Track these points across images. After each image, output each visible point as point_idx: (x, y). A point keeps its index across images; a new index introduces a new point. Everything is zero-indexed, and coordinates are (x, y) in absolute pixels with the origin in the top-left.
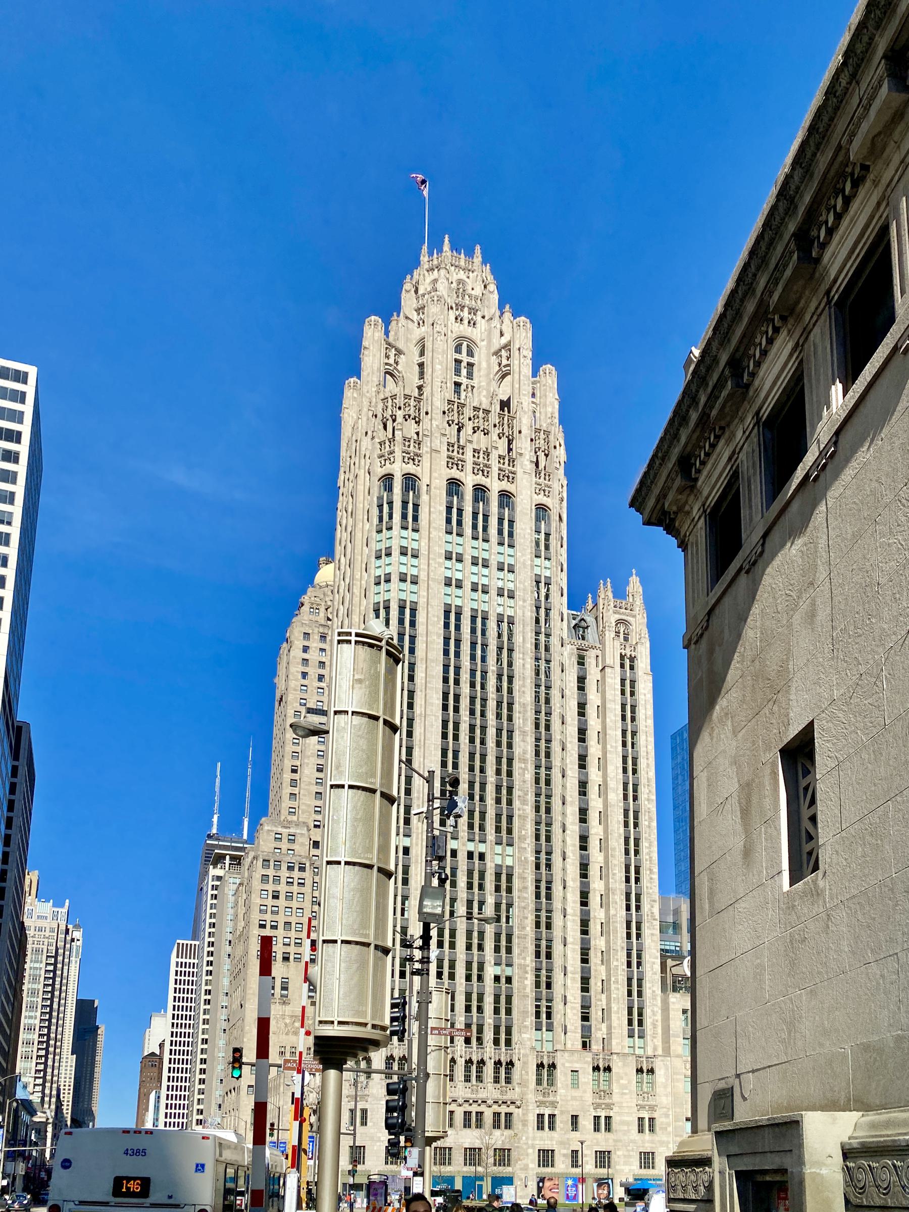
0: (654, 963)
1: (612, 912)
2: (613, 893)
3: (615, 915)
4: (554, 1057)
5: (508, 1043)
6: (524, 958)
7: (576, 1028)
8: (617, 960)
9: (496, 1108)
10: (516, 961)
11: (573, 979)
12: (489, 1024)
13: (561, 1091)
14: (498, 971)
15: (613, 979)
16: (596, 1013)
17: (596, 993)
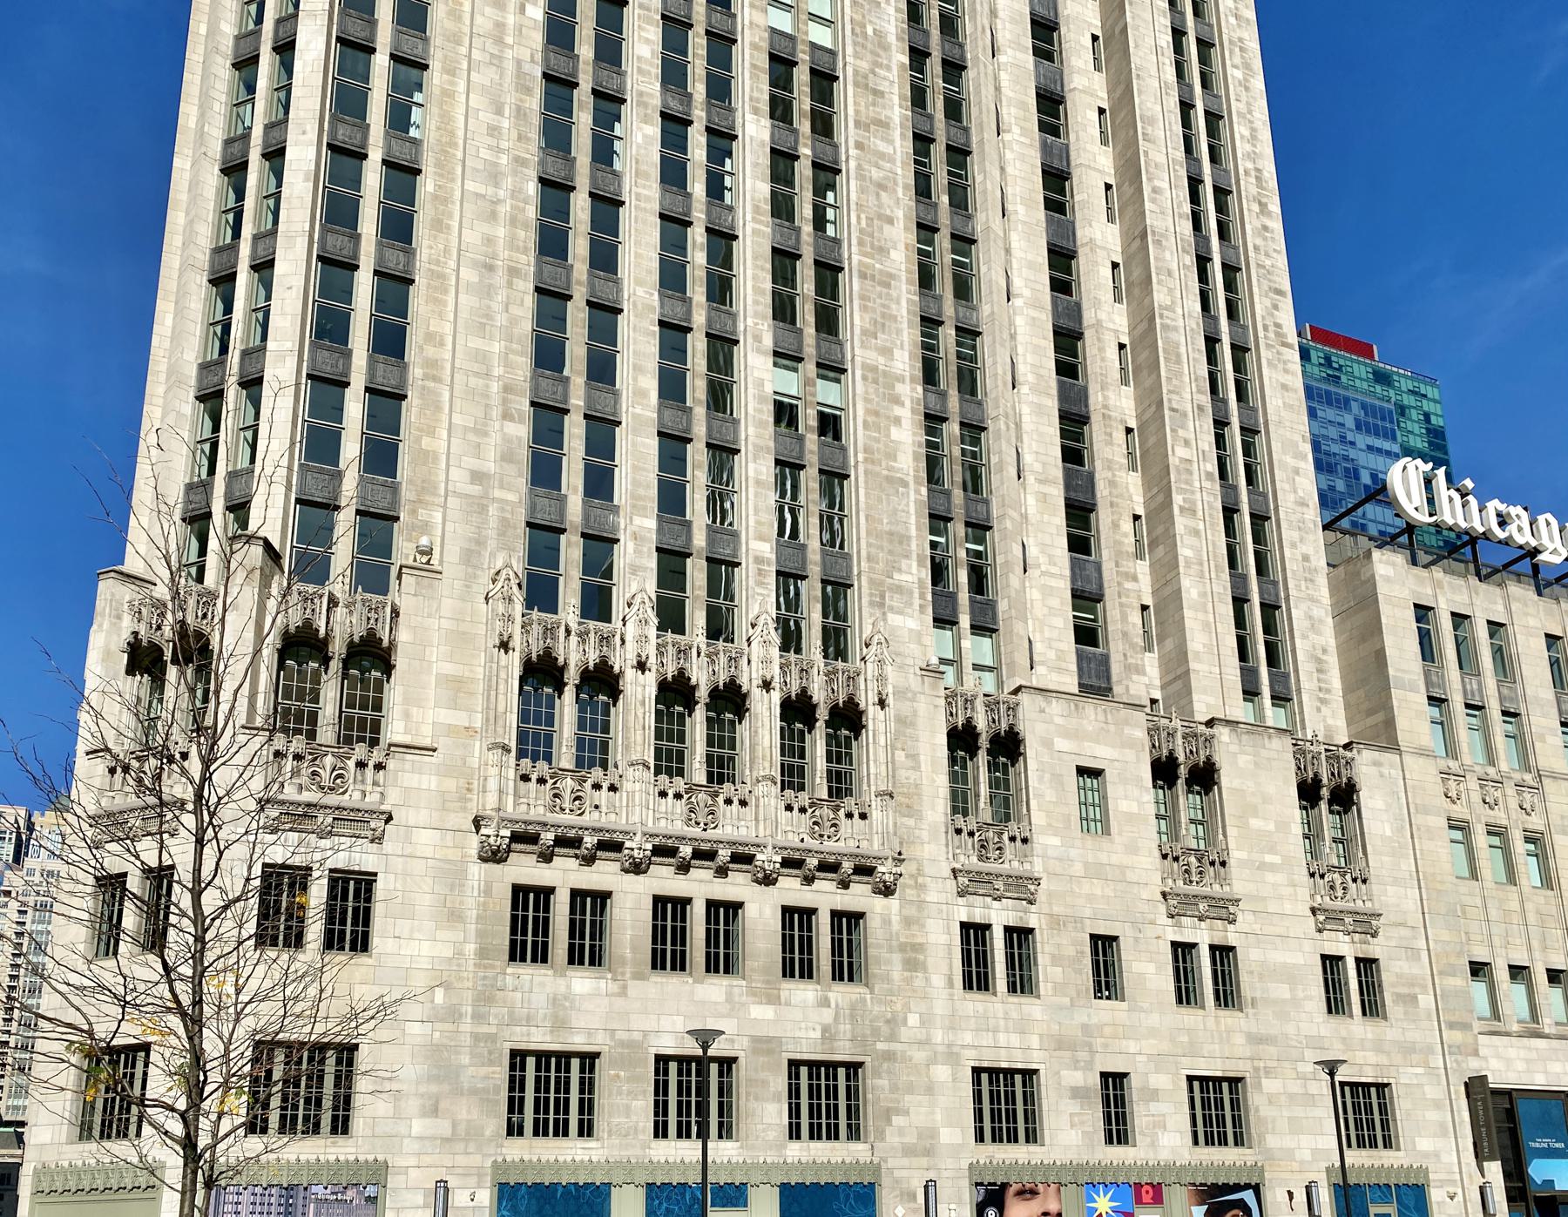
0: (1297, 472)
1: (1160, 296)
2: (1158, 243)
3: (1170, 308)
4: (1012, 709)
5: (835, 643)
6: (887, 352)
7: (1061, 655)
8: (1187, 443)
9: (791, 890)
10: (858, 351)
11: (1043, 498)
12: (759, 560)
13: (1044, 841)
14: (789, 383)
15: (1178, 499)
16: (1124, 618)
17: (1119, 553)
